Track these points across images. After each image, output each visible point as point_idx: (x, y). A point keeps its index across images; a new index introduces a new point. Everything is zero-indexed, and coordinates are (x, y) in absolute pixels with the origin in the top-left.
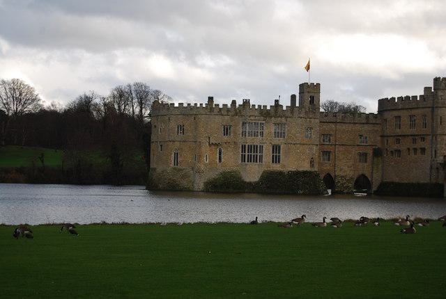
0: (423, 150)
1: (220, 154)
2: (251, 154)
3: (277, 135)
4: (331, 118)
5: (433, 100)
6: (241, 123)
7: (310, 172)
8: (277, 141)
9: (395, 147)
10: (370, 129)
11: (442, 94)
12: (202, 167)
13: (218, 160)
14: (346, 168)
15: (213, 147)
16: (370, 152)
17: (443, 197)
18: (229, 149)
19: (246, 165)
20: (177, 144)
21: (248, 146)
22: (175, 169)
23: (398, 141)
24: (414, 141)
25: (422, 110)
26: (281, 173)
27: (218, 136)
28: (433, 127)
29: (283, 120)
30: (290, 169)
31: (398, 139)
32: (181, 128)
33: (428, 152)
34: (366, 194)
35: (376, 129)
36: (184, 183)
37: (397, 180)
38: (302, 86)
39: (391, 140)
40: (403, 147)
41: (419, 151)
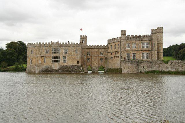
0: (118, 56)
1: (45, 60)
7: (77, 66)
8: (65, 55)
9: (111, 56)
11: (123, 36)
14: (95, 64)
17: (121, 73)
20: (31, 57)
23: (112, 54)
24: (116, 53)
26: (66, 66)
29: (67, 47)
31: (112, 53)
32: (32, 51)
33: (119, 57)
36: (33, 70)
37: (112, 67)
39: (110, 54)
40: (113, 56)
41: (117, 57)
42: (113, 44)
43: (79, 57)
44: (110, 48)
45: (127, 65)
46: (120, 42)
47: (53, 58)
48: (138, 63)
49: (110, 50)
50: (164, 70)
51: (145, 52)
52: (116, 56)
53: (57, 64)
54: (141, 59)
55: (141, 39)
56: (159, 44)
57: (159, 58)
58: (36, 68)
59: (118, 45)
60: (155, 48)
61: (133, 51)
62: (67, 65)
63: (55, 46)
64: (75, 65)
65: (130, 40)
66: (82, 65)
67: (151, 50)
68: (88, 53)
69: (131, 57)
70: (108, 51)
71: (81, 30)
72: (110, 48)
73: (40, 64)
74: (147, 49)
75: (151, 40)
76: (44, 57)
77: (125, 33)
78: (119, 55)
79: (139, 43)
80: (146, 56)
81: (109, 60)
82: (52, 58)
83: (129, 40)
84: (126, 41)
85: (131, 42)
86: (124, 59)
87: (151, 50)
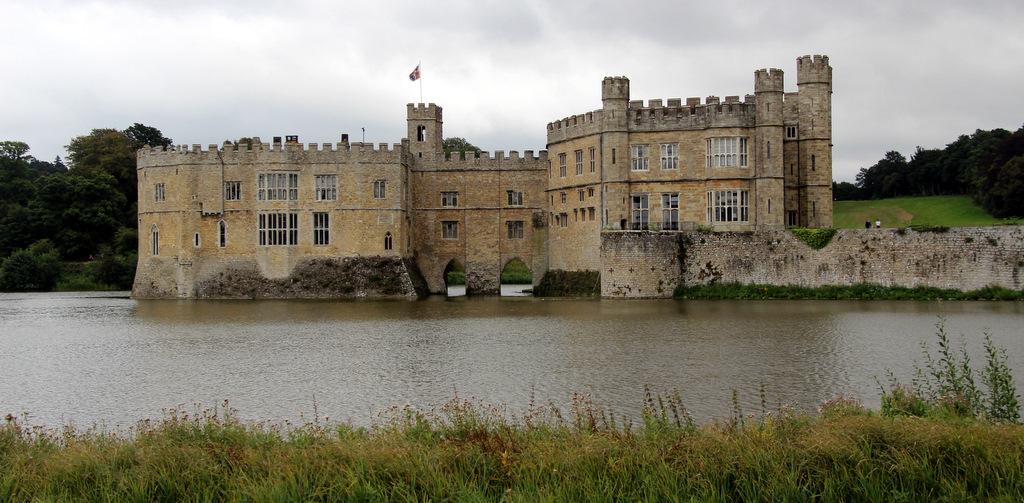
0: (592, 210)
1: (223, 230)
6: (257, 176)
8: (321, 207)
9: (560, 208)
13: (219, 243)
14: (484, 249)
15: (210, 221)
16: (528, 219)
18: (239, 223)
19: (267, 249)
21: (270, 216)
22: (154, 260)
25: (590, 138)
26: (329, 263)
29: (332, 168)
30: (345, 254)
35: (537, 178)
36: (163, 284)
37: (565, 268)
39: (557, 195)
40: (570, 211)
41: (587, 212)
42: (569, 148)
43: (393, 215)
45: (625, 255)
46: (598, 137)
47: (262, 225)
48: (680, 245)
50: (812, 282)
51: (724, 187)
52: (583, 210)
53: (282, 251)
56: (809, 144)
57: (810, 214)
58: (180, 275)
59: (592, 150)
60: (775, 166)
61: (662, 182)
64: (374, 254)
65: (648, 129)
66: (415, 252)
68: (449, 196)
69: (657, 214)
70: (547, 182)
71: (414, 76)
72: (556, 166)
74: (733, 174)
76: (212, 215)
77: (621, 90)
78: (592, 201)
79: (696, 142)
80: (726, 207)
82: (258, 223)
83: (641, 128)
84: (629, 132)
85: (655, 136)
86: (617, 224)
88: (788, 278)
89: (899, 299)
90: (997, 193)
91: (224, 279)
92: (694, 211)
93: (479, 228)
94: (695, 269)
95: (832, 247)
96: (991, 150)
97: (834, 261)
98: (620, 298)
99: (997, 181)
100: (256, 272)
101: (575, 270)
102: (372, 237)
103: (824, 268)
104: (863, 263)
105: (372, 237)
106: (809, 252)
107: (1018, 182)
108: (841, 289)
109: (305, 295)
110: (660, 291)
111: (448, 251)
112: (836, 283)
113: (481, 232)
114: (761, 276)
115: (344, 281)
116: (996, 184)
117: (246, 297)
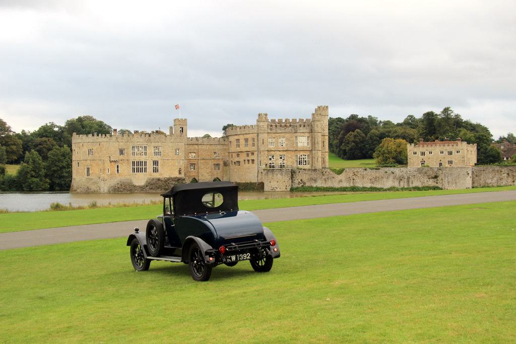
0: (253, 161)
2: (139, 167)
3: (156, 154)
4: (195, 142)
5: (258, 128)
8: (156, 158)
9: (237, 159)
10: (221, 148)
12: (106, 177)
14: (206, 174)
15: (113, 163)
16: (221, 163)
19: (136, 174)
22: (87, 178)
23: (238, 155)
24: (248, 155)
26: (159, 180)
27: (116, 156)
28: (258, 145)
32: (90, 151)
33: (256, 162)
34: (172, 198)
35: (225, 148)
36: (93, 188)
37: (238, 181)
38: (175, 120)
41: (251, 162)
43: (181, 162)
44: (235, 143)
46: (256, 135)
49: (233, 148)
50: (337, 185)
51: (302, 153)
52: (248, 160)
54: (295, 165)
55: (294, 129)
58: (102, 184)
61: (279, 151)
62: (160, 177)
63: (139, 141)
67: (312, 150)
73: (108, 175)
75: (312, 132)
76: (115, 161)
77: (265, 118)
78: (254, 157)
81: (232, 166)
82: (132, 164)
83: (272, 132)
84: (268, 133)
85: (278, 135)
86: (264, 166)
87: (312, 150)
88: (329, 184)
89: (366, 191)
90: (344, 148)
91: (119, 186)
92: (290, 162)
93: (203, 166)
94: (296, 182)
95: (343, 174)
96: (338, 128)
97: (343, 179)
98: (273, 191)
99: (343, 143)
100: (132, 183)
101: (244, 182)
102: (175, 170)
103: (341, 181)
104: (353, 179)
105: (175, 170)
106: (336, 176)
107: (353, 144)
108: (347, 188)
109: (150, 191)
110: (286, 189)
111: (192, 175)
112: (345, 186)
113: (204, 168)
114: (319, 184)
115: (165, 186)
116: (343, 144)
117: (129, 192)
